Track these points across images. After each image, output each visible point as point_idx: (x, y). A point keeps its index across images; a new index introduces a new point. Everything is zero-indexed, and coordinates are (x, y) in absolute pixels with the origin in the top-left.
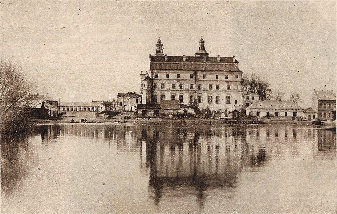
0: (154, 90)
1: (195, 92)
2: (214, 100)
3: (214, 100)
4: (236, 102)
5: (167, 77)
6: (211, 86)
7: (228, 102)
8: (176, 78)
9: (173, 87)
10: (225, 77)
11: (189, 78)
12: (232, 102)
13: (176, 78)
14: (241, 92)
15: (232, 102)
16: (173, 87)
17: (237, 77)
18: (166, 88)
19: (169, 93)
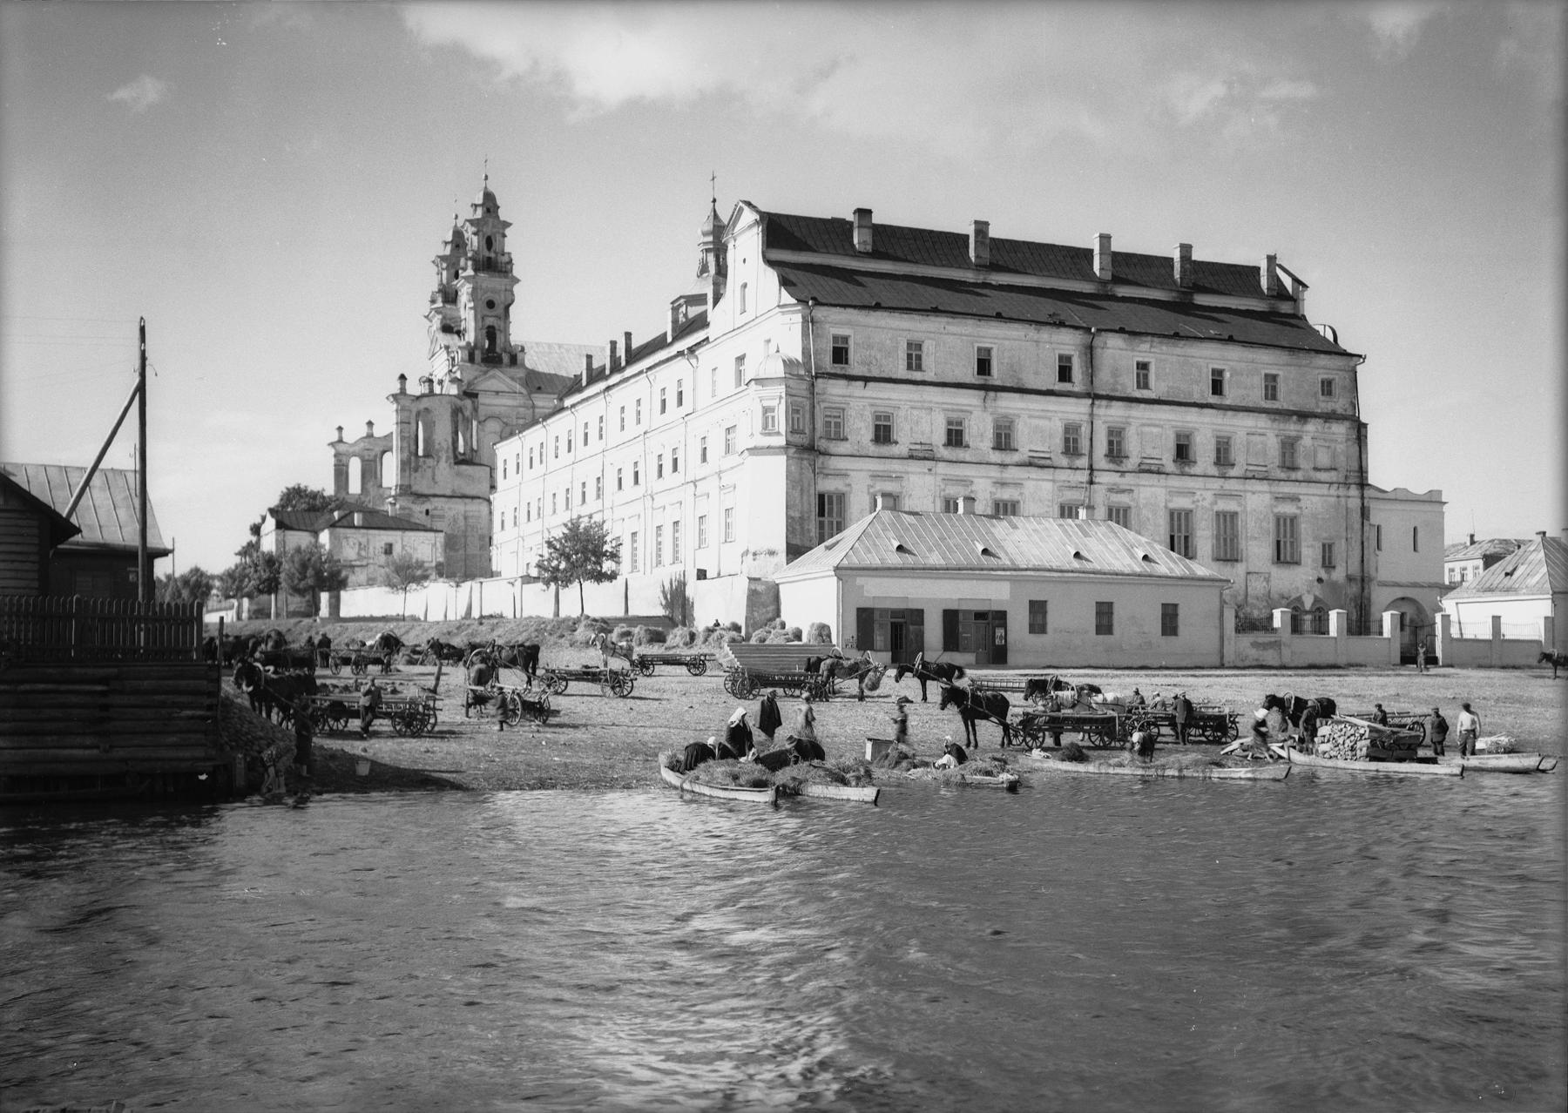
0: (826, 454)
1: (1091, 482)
2: (1204, 540)
3: (1204, 540)
4: (1327, 550)
5: (909, 367)
6: (1183, 452)
7: (1284, 554)
8: (970, 376)
9: (955, 438)
10: (1258, 383)
11: (1050, 380)
12: (1309, 552)
13: (970, 376)
14: (1354, 491)
15: (1309, 552)
16: (955, 438)
17: (1327, 387)
18: (901, 449)
19: (929, 479)
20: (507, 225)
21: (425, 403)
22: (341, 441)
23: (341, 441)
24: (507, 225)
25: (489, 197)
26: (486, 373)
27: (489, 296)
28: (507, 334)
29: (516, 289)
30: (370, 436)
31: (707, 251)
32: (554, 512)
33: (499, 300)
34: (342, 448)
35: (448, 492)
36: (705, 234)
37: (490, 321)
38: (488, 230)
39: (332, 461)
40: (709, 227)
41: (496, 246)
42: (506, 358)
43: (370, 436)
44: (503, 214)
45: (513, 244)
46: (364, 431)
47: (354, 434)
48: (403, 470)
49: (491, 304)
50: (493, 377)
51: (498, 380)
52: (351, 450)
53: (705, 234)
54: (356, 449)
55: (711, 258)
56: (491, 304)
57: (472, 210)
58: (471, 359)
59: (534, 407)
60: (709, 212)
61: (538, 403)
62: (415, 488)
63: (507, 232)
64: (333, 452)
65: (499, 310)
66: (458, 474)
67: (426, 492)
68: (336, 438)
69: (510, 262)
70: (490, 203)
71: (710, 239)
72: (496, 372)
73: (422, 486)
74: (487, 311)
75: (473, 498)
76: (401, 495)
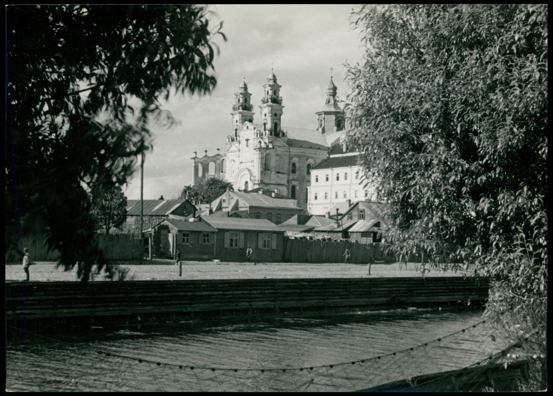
20: (280, 86)
21: (268, 151)
22: (196, 157)
23: (196, 157)
24: (280, 86)
25: (274, 76)
26: (275, 139)
27: (275, 112)
28: (280, 124)
29: (284, 110)
30: (206, 156)
31: (330, 95)
32: (356, 197)
33: (278, 113)
34: (197, 160)
35: (274, 183)
36: (330, 89)
37: (275, 121)
38: (275, 88)
39: (193, 165)
40: (332, 87)
41: (277, 94)
42: (281, 134)
43: (206, 156)
44: (278, 82)
45: (282, 93)
46: (204, 154)
47: (200, 155)
48: (261, 175)
49: (276, 115)
50: (278, 141)
51: (280, 142)
52: (200, 161)
53: (330, 89)
54: (202, 160)
55: (331, 98)
56: (276, 115)
57: (267, 81)
58: (271, 134)
59: (289, 152)
60: (330, 81)
61: (291, 150)
62: (265, 181)
63: (280, 89)
64: (193, 161)
65: (278, 118)
66: (278, 177)
67: (268, 182)
68: (194, 156)
69: (281, 100)
70: (275, 79)
71: (332, 91)
72: (279, 139)
73: (267, 181)
74: (275, 118)
75: (282, 185)
76: (261, 183)
